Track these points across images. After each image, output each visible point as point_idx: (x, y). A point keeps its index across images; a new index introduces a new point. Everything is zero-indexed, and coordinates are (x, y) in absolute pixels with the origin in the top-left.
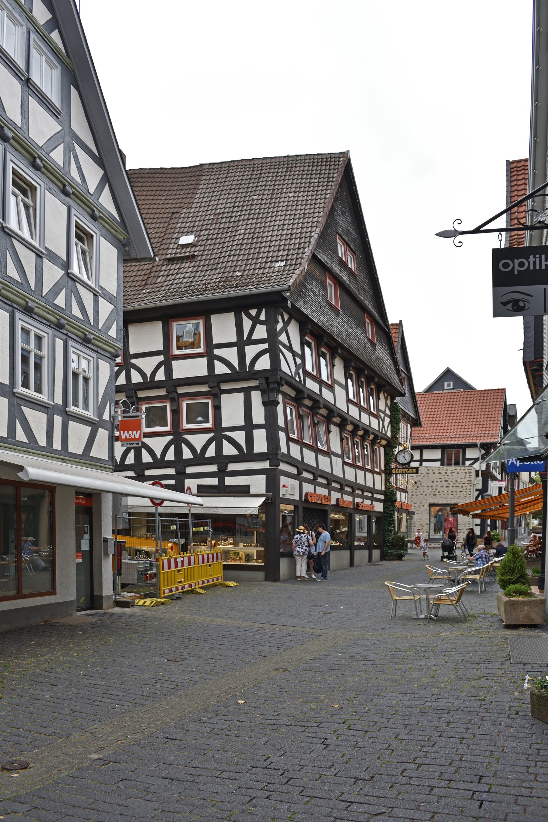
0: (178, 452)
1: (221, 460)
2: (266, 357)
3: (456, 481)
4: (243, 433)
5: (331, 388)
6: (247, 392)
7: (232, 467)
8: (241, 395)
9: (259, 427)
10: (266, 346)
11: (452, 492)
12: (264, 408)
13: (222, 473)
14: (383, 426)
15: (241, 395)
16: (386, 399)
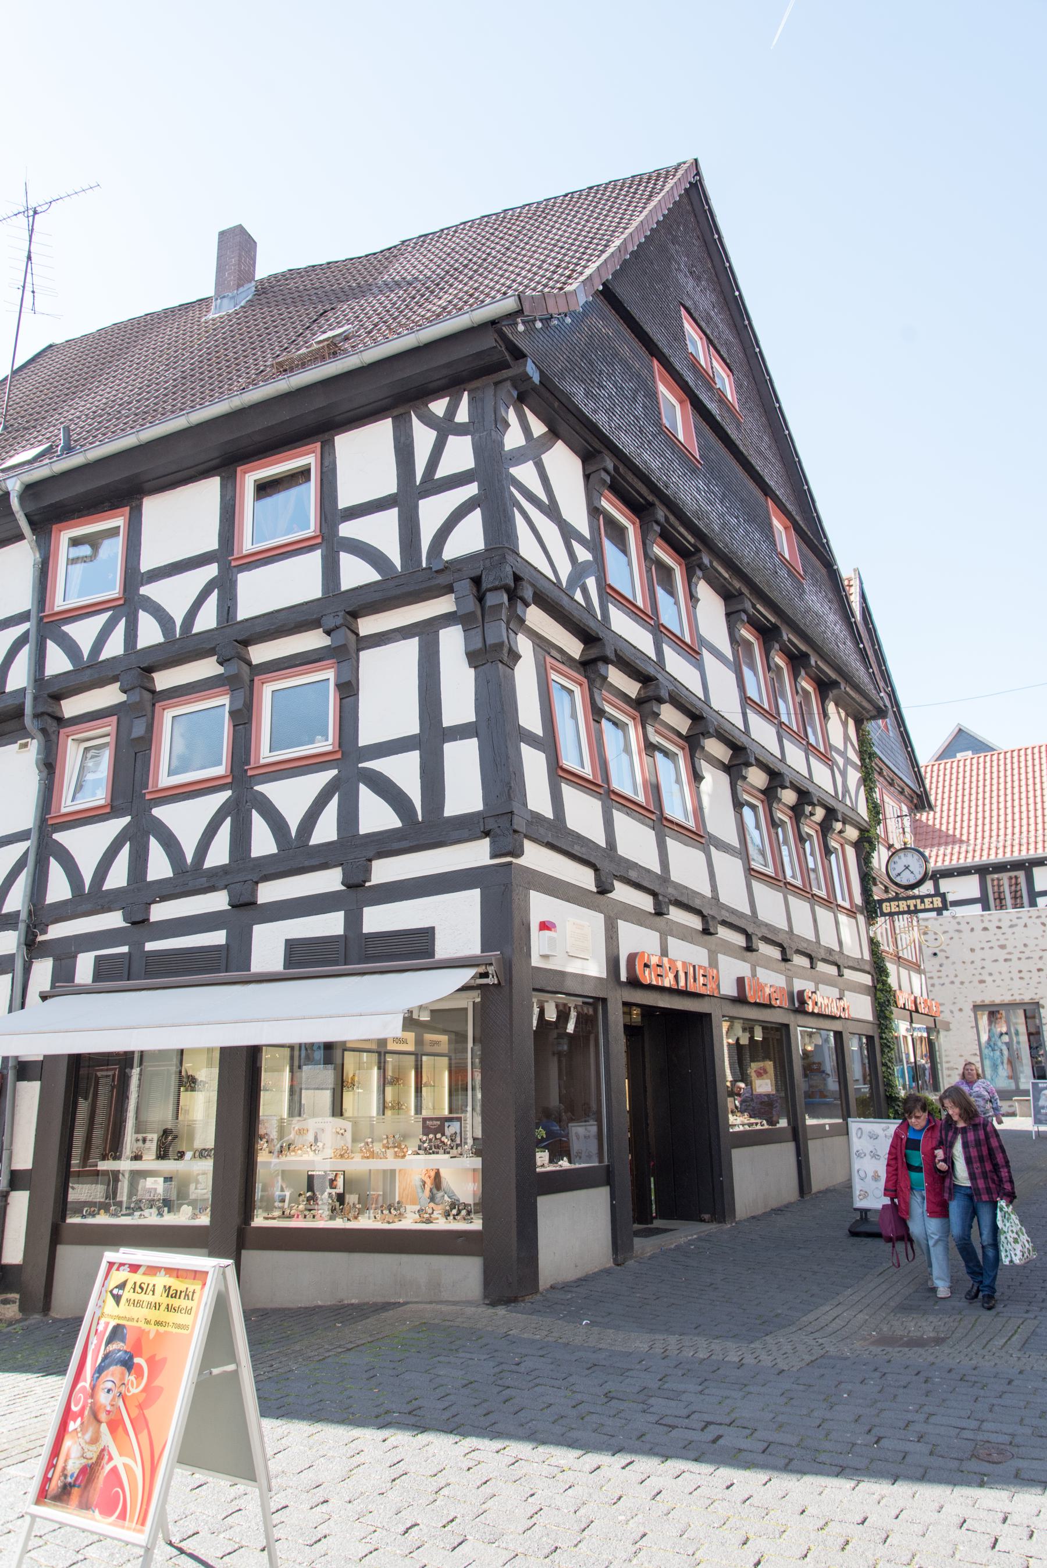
0: (241, 839)
1: (355, 852)
2: (475, 519)
3: (1025, 945)
5: (692, 652)
6: (427, 633)
7: (385, 871)
8: (411, 647)
9: (460, 732)
10: (472, 489)
11: (1020, 972)
12: (472, 672)
13: (358, 893)
14: (846, 790)
15: (411, 647)
16: (845, 724)
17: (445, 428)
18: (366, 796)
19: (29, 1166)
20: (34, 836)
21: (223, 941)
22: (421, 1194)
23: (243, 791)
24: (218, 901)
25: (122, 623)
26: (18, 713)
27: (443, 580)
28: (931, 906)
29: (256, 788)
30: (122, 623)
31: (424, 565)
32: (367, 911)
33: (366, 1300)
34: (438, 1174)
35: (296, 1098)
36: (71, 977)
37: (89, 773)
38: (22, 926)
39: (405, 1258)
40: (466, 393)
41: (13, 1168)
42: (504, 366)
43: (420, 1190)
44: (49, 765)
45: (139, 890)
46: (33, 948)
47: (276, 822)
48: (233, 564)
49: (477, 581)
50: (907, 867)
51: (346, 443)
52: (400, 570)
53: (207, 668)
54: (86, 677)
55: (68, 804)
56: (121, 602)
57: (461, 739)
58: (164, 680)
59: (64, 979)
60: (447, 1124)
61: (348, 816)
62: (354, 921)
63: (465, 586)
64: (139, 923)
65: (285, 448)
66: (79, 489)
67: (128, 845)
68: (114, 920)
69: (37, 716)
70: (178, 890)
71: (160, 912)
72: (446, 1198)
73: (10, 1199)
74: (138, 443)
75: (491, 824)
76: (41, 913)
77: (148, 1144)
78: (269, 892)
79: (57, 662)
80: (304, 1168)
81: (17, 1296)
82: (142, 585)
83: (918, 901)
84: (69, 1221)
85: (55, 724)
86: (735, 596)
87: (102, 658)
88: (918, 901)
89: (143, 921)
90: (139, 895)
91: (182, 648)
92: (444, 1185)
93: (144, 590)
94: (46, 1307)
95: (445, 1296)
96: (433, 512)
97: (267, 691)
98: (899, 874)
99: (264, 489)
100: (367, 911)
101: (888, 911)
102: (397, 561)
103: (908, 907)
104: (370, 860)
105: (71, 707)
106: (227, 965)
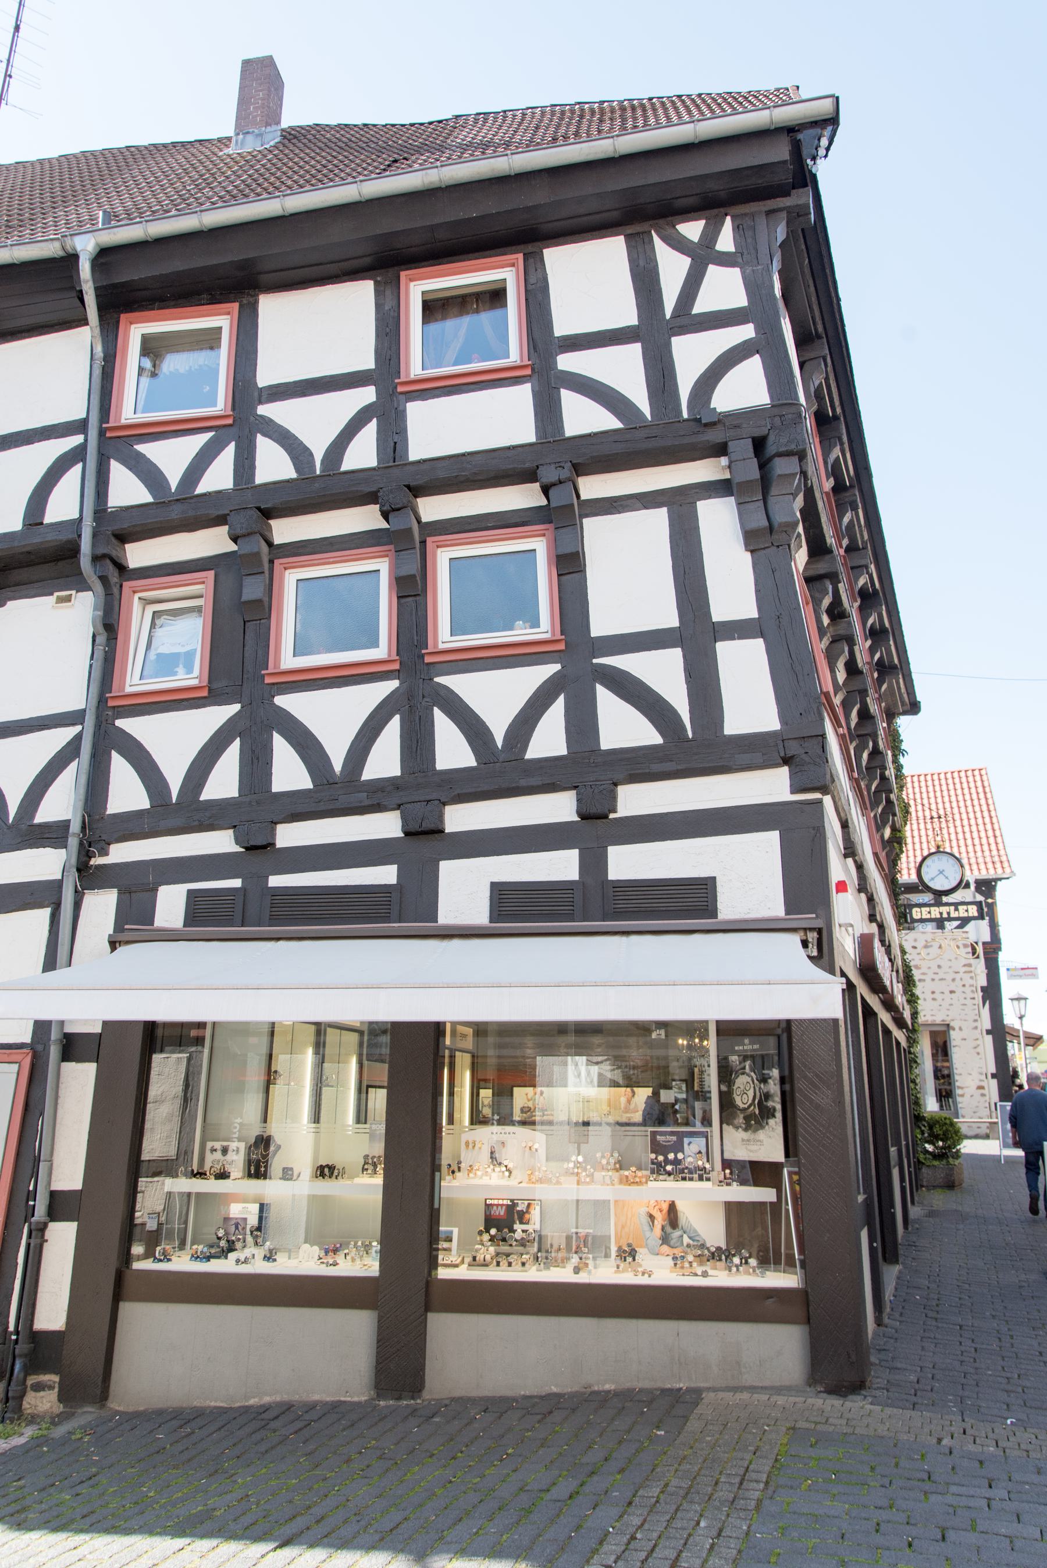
1: (590, 772)
3: (939, 967)
4: (674, 657)
7: (635, 800)
11: (933, 993)
15: (659, 519)
17: (702, 256)
18: (605, 699)
19: (78, 1185)
20: (90, 720)
21: (393, 880)
22: (648, 1234)
23: (418, 685)
24: (386, 825)
25: (230, 450)
26: (69, 551)
27: (715, 436)
28: (928, 916)
29: (437, 679)
30: (230, 450)
31: (685, 415)
32: (613, 851)
33: (628, 1385)
34: (672, 1208)
35: (364, 1095)
36: (148, 916)
37: (171, 641)
38: (73, 842)
39: (685, 1327)
40: (728, 219)
41: (52, 1188)
42: (783, 191)
43: (646, 1228)
44: (110, 628)
45: (258, 803)
46: (88, 875)
47: (473, 728)
48: (400, 389)
49: (759, 444)
50: (941, 872)
51: (561, 261)
52: (650, 419)
53: (363, 519)
54: (175, 513)
55: (135, 680)
56: (230, 421)
57: (740, 638)
58: (286, 530)
59: (134, 923)
60: (686, 1140)
61: (582, 724)
62: (594, 863)
63: (743, 448)
64: (259, 849)
65: (477, 254)
66: (176, 264)
67: (237, 743)
68: (221, 842)
69: (96, 559)
70: (322, 807)
71: (290, 835)
72: (686, 1240)
73: (48, 1234)
74: (280, 213)
75: (794, 748)
76: (97, 828)
77: (231, 1156)
78: (459, 818)
79: (126, 490)
80: (480, 1197)
81: (56, 1378)
82: (261, 403)
83: (952, 908)
84: (137, 1265)
85: (116, 573)
86: (860, 550)
87: (200, 490)
88: (952, 908)
89: (264, 847)
90: (257, 811)
91: (322, 487)
92: (682, 1221)
93: (262, 410)
94: (103, 1396)
95: (748, 1379)
96: (692, 355)
97: (443, 558)
98: (933, 879)
99: (435, 308)
100: (613, 851)
101: (919, 917)
102: (644, 406)
103: (941, 914)
104: (616, 785)
105: (140, 554)
106: (402, 911)
